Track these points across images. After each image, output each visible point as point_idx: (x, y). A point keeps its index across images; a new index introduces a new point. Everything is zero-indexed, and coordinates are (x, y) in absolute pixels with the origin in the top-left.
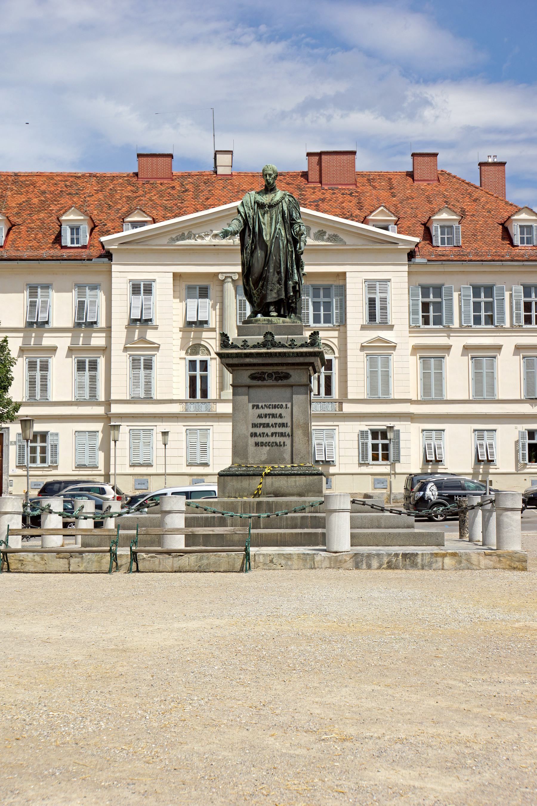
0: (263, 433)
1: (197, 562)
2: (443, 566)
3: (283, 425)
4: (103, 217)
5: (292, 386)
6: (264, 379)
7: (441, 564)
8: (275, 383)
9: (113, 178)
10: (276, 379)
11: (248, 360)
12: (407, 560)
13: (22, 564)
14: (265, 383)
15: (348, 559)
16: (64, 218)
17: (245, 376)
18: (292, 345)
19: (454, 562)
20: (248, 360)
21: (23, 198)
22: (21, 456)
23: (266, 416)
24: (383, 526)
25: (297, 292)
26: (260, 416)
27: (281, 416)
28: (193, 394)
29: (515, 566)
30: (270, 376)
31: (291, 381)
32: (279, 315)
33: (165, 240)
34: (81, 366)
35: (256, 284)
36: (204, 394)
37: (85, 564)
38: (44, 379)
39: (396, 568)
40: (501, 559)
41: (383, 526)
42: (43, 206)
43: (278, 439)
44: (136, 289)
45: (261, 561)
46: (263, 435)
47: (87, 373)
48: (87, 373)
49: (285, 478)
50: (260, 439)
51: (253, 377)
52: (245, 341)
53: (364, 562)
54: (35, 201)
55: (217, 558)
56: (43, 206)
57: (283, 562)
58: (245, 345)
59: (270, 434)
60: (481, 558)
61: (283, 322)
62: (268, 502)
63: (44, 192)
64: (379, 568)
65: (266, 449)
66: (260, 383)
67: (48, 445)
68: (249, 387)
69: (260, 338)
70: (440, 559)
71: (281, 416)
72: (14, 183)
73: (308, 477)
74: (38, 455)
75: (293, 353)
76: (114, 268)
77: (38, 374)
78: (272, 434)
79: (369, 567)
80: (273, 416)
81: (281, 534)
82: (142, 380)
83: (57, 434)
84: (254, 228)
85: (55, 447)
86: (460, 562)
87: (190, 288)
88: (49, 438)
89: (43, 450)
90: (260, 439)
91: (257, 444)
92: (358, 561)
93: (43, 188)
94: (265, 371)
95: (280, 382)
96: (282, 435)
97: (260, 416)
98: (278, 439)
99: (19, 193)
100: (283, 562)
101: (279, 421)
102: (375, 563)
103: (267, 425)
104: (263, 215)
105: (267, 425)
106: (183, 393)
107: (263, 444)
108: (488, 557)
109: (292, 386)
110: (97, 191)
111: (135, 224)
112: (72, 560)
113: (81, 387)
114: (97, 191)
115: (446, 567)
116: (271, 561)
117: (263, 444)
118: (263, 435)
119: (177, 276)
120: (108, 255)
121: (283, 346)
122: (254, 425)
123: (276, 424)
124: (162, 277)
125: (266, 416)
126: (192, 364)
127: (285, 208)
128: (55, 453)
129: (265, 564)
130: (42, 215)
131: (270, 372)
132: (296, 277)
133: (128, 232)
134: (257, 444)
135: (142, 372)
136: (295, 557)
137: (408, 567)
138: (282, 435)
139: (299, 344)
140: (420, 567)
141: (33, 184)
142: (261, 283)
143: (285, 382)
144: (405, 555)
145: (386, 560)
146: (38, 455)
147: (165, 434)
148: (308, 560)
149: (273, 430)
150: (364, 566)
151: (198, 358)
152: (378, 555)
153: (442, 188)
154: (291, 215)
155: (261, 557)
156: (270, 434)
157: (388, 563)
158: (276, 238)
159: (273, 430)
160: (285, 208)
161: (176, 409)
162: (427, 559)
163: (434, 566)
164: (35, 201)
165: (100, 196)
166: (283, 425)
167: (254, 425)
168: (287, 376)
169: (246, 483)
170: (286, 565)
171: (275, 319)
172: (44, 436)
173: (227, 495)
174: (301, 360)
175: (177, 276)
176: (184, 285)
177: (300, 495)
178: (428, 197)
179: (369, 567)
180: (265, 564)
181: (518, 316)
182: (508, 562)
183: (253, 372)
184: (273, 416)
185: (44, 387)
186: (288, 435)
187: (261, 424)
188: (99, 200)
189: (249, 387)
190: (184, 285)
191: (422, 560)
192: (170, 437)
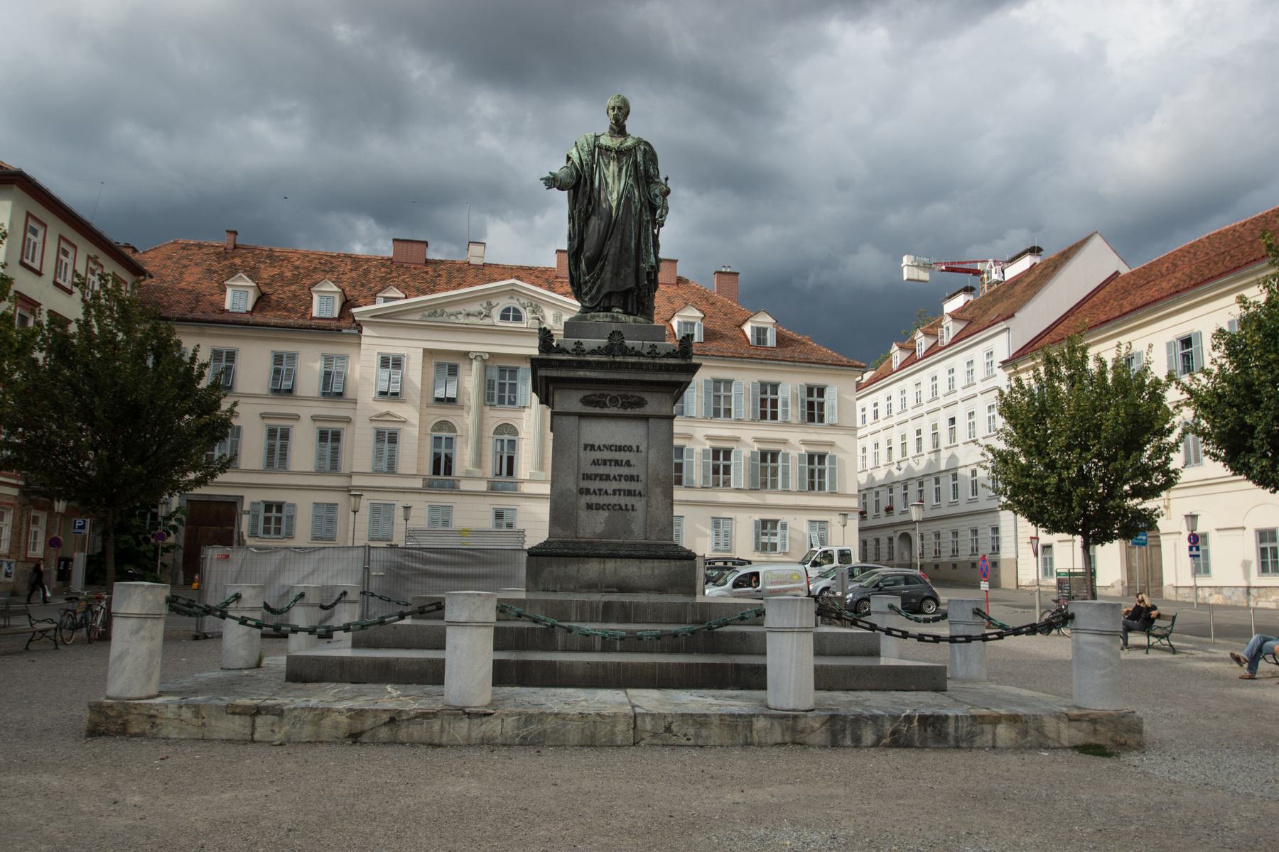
0: (600, 490)
1: (518, 729)
2: (994, 740)
3: (631, 478)
4: (355, 293)
5: (646, 418)
6: (604, 406)
7: (990, 736)
8: (621, 411)
9: (368, 260)
10: (624, 406)
11: (581, 374)
12: (929, 730)
13: (153, 725)
14: (606, 411)
15: (817, 725)
16: (315, 289)
17: (571, 401)
18: (653, 353)
19: (1013, 735)
20: (581, 374)
21: (276, 271)
22: (254, 527)
23: (605, 462)
24: (828, 650)
25: (654, 284)
26: (595, 463)
27: (628, 464)
28: (436, 471)
29: (1122, 740)
30: (614, 401)
31: (648, 410)
32: (626, 312)
33: (417, 317)
34: (323, 436)
35: (591, 265)
36: (448, 471)
37: (286, 728)
38: (284, 448)
39: (908, 745)
40: (1098, 727)
41: (828, 650)
42: (295, 279)
43: (623, 500)
44: (385, 362)
45: (649, 727)
46: (600, 492)
47: (329, 444)
48: (329, 444)
49: (637, 562)
50: (594, 499)
51: (586, 401)
52: (578, 343)
53: (848, 732)
54: (288, 274)
55: (560, 722)
56: (295, 279)
57: (691, 731)
58: (579, 349)
59: (610, 491)
60: (1062, 726)
61: (635, 321)
62: (623, 604)
63: (297, 268)
64: (876, 744)
65: (604, 514)
66: (597, 410)
67: (284, 516)
68: (582, 416)
69: (603, 342)
70: (988, 728)
71: (628, 464)
72: (268, 257)
73: (673, 563)
74: (273, 525)
75: (654, 364)
76: (364, 340)
77: (278, 443)
78: (614, 492)
79: (857, 743)
80: (617, 463)
81: (661, 665)
82: (386, 455)
83: (294, 505)
84: (592, 183)
85: (291, 518)
86: (1025, 733)
87: (439, 365)
88: (285, 509)
89: (279, 520)
90: (594, 499)
91: (590, 507)
92: (841, 731)
93: (297, 263)
94: (605, 392)
95: (629, 411)
96: (629, 493)
97: (595, 463)
98: (623, 500)
99: (272, 265)
100: (691, 731)
101: (625, 471)
102: (868, 736)
103: (608, 478)
104: (607, 166)
105: (608, 478)
106: (427, 468)
107: (599, 507)
108: (1074, 724)
109: (646, 418)
110: (351, 270)
111: (387, 299)
112: (260, 720)
113: (321, 457)
114: (351, 270)
115: (1000, 743)
116: (668, 729)
117: (599, 507)
118: (600, 492)
119: (428, 353)
120: (359, 326)
121: (639, 354)
122: (587, 477)
123: (620, 476)
124: (412, 348)
125: (605, 462)
126: (438, 439)
127: (640, 158)
128: (291, 525)
129: (655, 735)
130: (293, 288)
131: (614, 394)
132: (653, 259)
133: (380, 304)
134: (590, 507)
135: (386, 446)
136: (716, 721)
137: (930, 742)
138: (629, 493)
139: (663, 352)
140: (952, 743)
141: (288, 260)
142: (599, 265)
143: (637, 411)
144: (924, 719)
145: (888, 728)
146: (273, 525)
147: (407, 508)
148: (740, 728)
149: (615, 485)
150: (848, 742)
151: (444, 434)
152: (875, 719)
153: (680, 292)
154: (646, 171)
155: (648, 720)
156: (610, 491)
157: (893, 733)
158: (626, 199)
159: (615, 485)
160: (640, 158)
161: (418, 483)
162: (965, 727)
163: (978, 741)
164: (288, 274)
165: (354, 274)
166: (631, 478)
167: (587, 477)
168: (641, 403)
169: (573, 569)
170: (697, 736)
171: (622, 317)
172: (280, 507)
173: (541, 586)
174: (665, 377)
175: (428, 353)
176: (433, 362)
177: (661, 590)
178: (669, 298)
179: (857, 743)
180: (655, 735)
181: (754, 411)
182: (1110, 734)
183: (588, 393)
184: (617, 463)
185: (284, 457)
186: (640, 494)
187: (596, 475)
188: (353, 278)
189: (582, 416)
190: (433, 362)
191: (956, 729)
192: (412, 512)
